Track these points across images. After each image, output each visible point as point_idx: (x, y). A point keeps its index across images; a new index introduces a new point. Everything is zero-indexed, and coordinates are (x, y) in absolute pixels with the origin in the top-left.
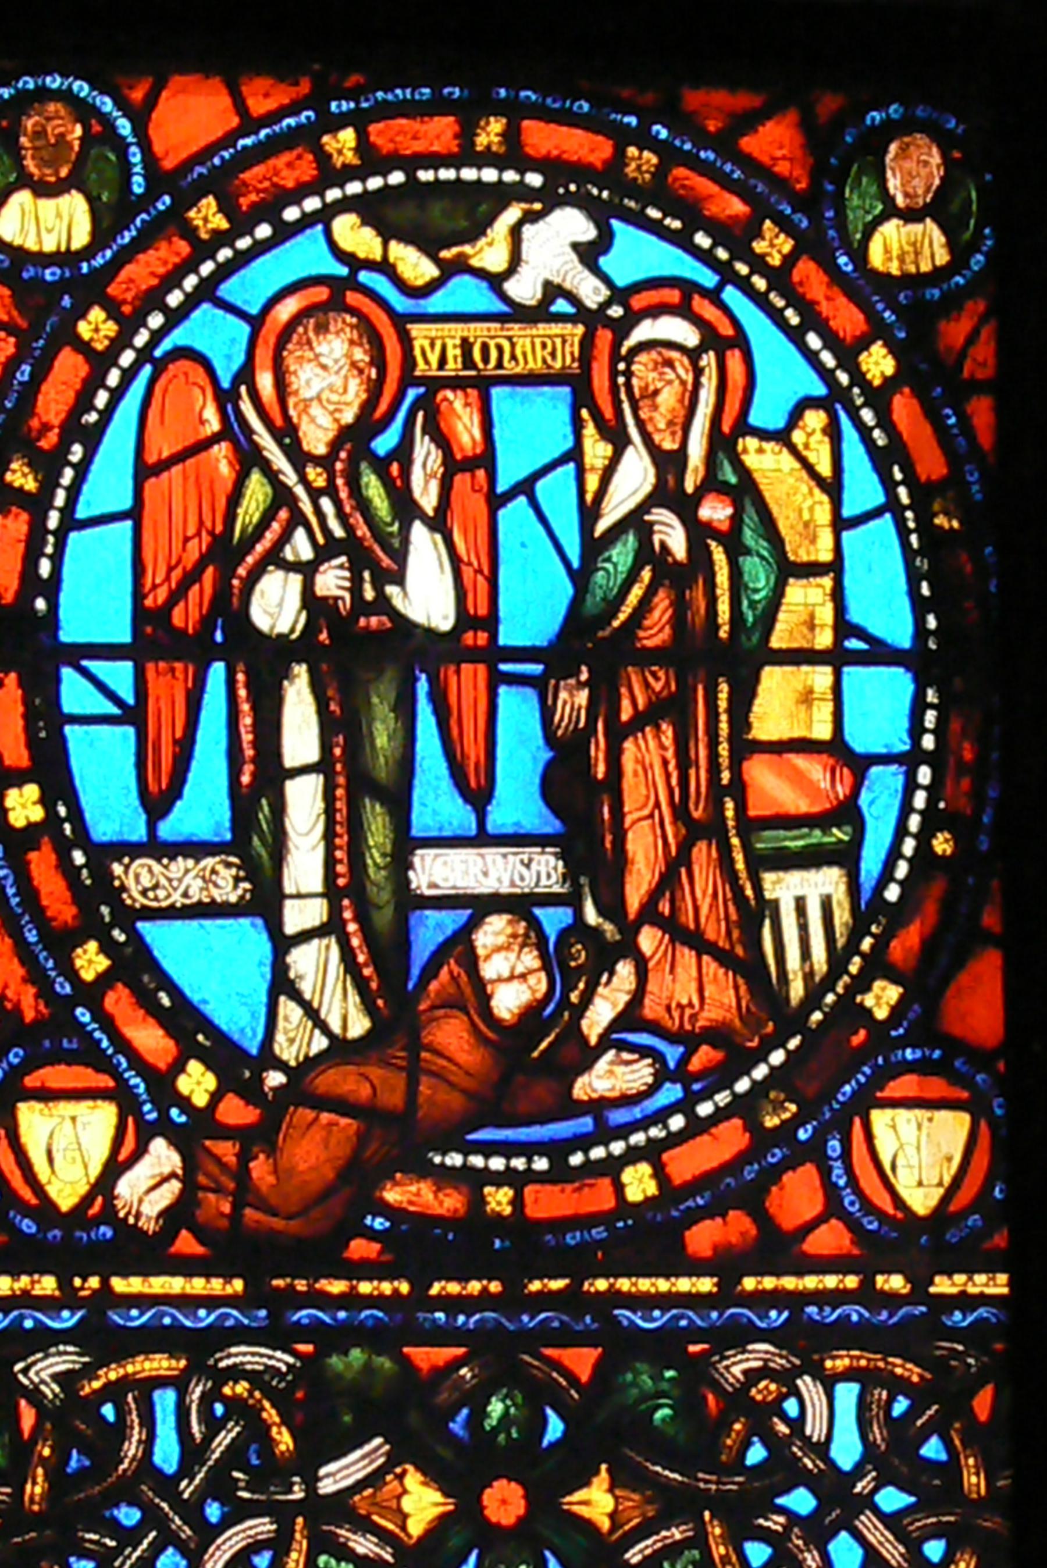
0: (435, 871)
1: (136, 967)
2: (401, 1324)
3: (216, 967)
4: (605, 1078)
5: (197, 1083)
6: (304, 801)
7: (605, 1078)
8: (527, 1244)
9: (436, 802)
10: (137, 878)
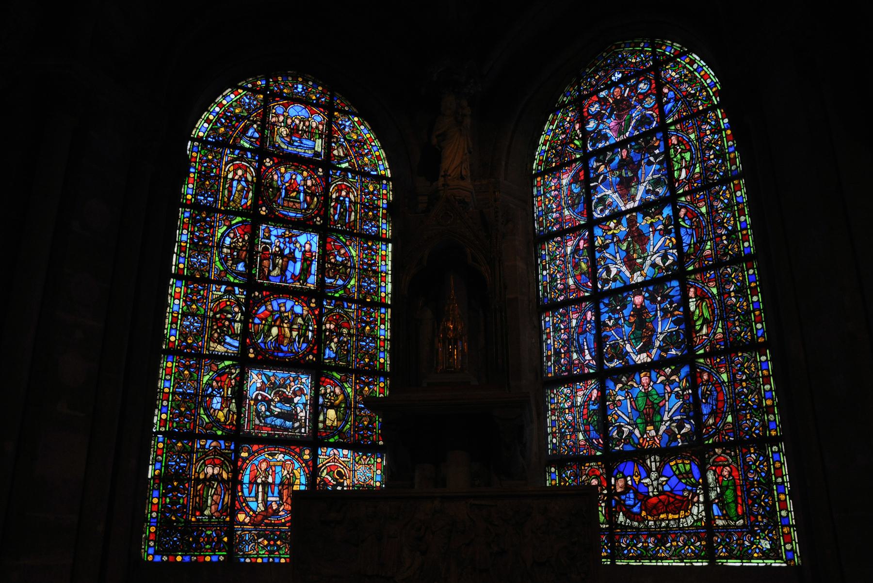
0: (269, 499)
1: (247, 505)
2: (265, 530)
3: (253, 505)
4: (281, 513)
5: (251, 513)
6: (260, 494)
7: (281, 513)
8: (275, 525)
9: (270, 494)
10: (248, 499)
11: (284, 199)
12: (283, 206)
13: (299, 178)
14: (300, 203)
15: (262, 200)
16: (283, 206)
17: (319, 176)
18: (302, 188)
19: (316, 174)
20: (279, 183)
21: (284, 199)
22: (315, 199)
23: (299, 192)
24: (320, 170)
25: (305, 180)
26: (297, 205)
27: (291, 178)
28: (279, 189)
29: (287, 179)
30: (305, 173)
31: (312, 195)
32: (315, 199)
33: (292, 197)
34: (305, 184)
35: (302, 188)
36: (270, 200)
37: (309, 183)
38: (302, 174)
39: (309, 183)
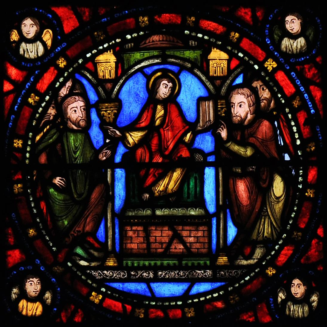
11: (123, 219)
12: (123, 255)
13: (191, 89)
14: (205, 220)
15: (23, 242)
16: (123, 255)
17: (287, 60)
18: (206, 143)
19: (274, 51)
20: (96, 134)
21: (123, 219)
22: (278, 187)
23: (194, 168)
24: (293, 24)
25: (218, 93)
26: (192, 236)
27: (151, 101)
28: (96, 171)
29: (132, 107)
30: (218, 58)
31: (260, 172)
32: (278, 187)
33: (166, 200)
34: (224, 117)
35: (206, 143)
36: (59, 235)
37: (241, 106)
38: (201, 66)
39: (241, 106)
